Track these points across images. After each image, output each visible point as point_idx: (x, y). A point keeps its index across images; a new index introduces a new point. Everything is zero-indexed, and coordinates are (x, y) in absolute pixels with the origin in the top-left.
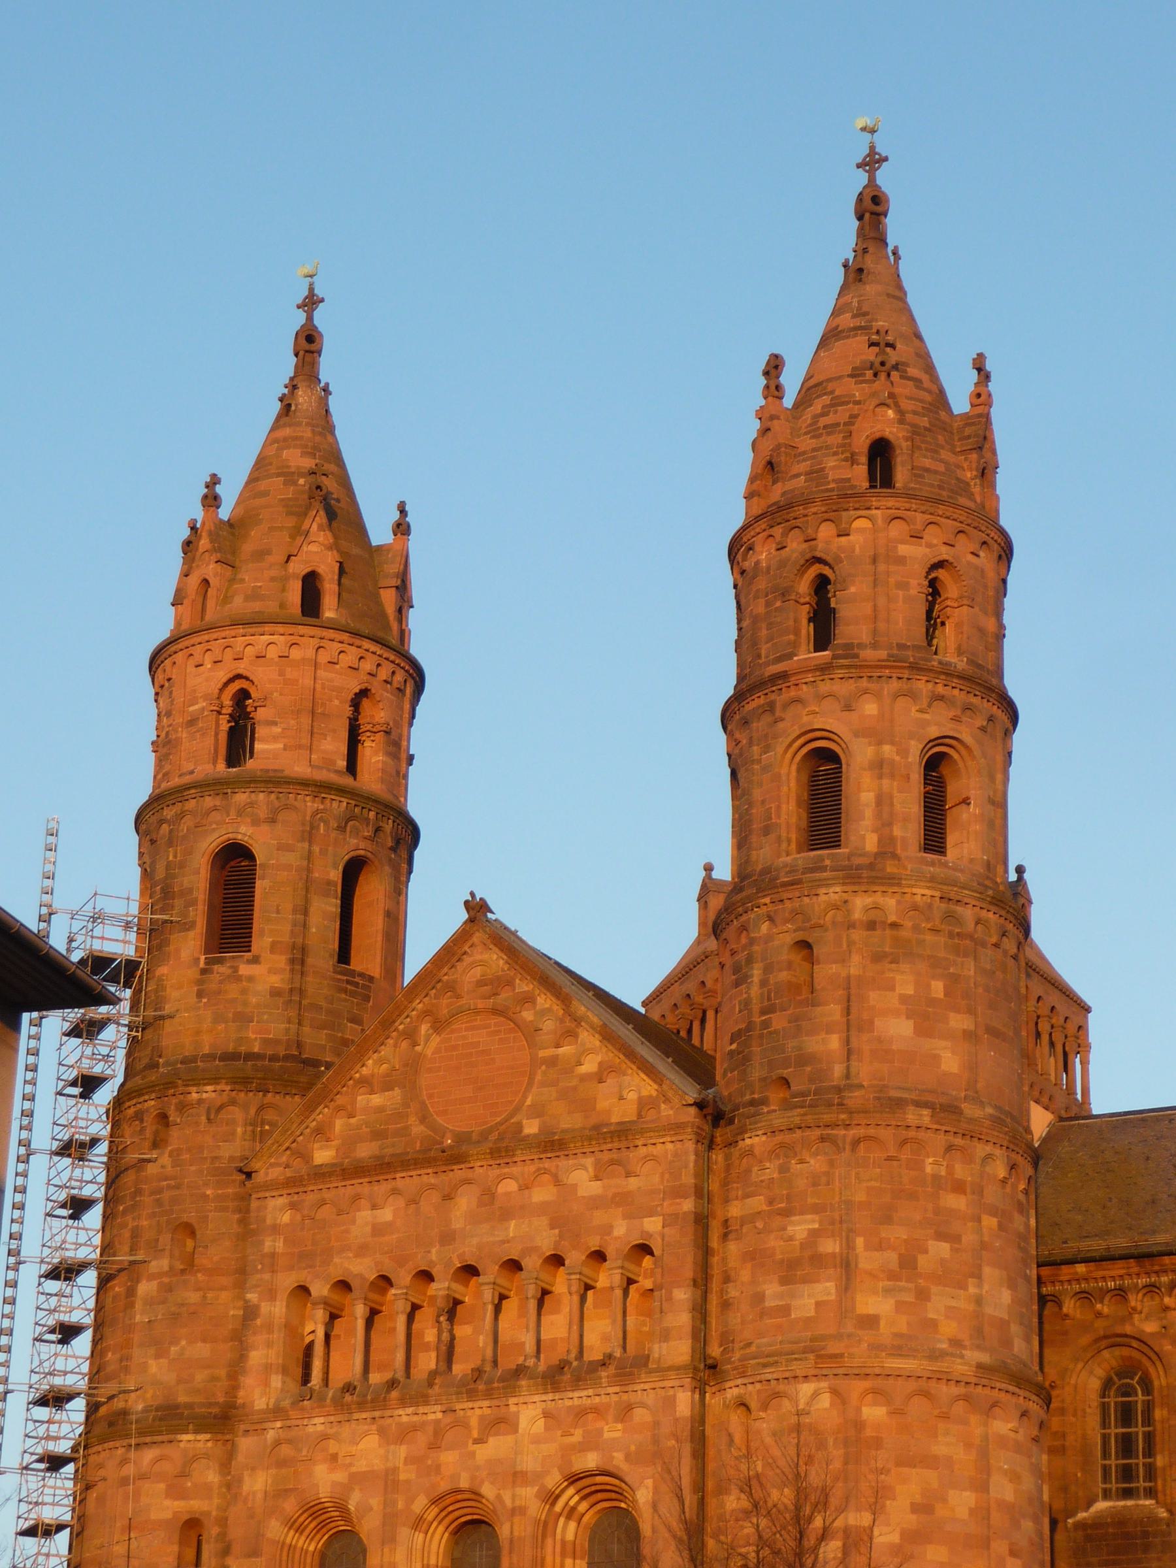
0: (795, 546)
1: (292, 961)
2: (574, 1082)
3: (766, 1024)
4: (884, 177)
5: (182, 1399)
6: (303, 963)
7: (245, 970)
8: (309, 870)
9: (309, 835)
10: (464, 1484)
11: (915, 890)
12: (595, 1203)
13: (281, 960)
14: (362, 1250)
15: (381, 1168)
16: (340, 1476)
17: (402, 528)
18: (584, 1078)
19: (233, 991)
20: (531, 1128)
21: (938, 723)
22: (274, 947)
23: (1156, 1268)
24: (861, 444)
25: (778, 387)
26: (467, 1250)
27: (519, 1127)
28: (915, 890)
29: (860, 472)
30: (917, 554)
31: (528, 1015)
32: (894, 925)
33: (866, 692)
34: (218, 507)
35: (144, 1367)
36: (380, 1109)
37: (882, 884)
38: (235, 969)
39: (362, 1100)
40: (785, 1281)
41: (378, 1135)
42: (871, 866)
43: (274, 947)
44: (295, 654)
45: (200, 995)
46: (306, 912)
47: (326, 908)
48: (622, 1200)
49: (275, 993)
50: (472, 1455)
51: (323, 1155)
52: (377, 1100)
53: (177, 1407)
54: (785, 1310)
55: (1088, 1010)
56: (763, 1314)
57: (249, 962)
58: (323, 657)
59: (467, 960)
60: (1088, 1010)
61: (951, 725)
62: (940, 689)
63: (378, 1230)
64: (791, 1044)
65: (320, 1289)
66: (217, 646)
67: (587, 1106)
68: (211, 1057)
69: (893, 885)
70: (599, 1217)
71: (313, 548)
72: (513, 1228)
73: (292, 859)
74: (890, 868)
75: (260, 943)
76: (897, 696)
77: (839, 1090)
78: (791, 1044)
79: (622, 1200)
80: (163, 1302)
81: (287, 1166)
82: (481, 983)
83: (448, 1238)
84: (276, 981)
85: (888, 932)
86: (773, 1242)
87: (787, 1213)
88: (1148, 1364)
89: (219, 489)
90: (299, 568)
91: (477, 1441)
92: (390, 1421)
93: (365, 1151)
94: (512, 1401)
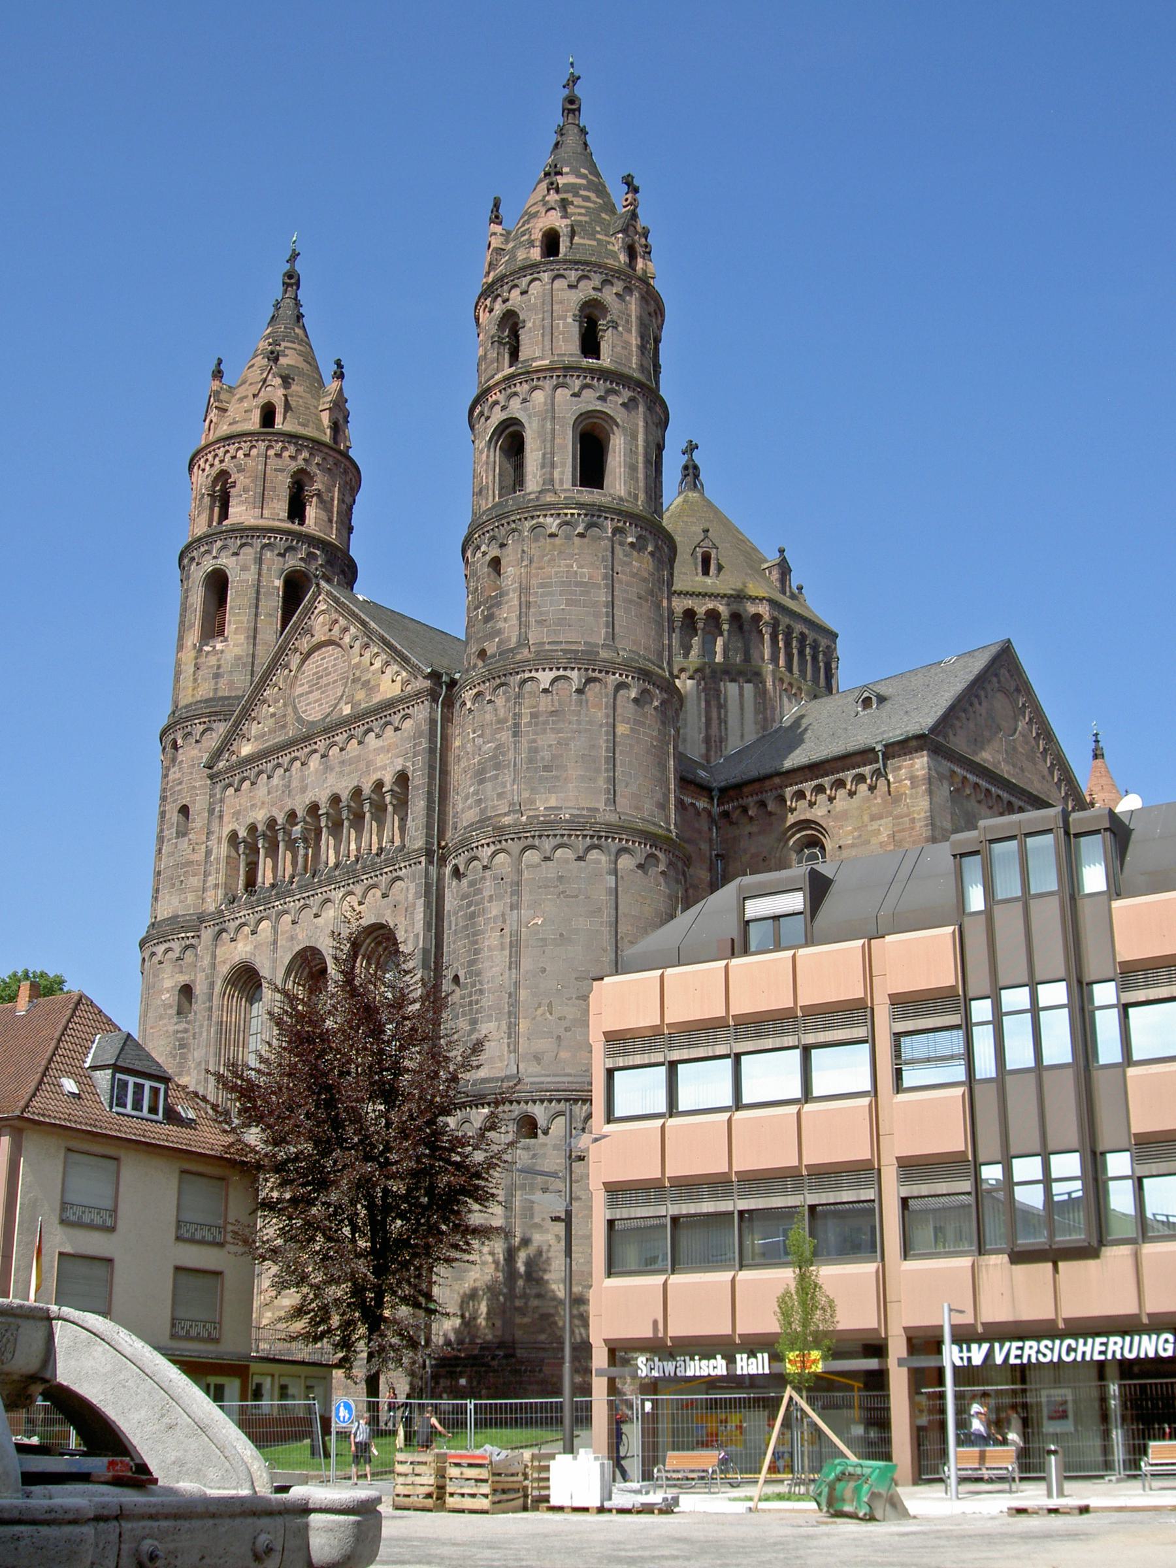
0: (499, 308)
1: (248, 638)
2: (370, 675)
4: (578, 90)
6: (255, 638)
7: (219, 646)
8: (259, 581)
9: (260, 561)
11: (566, 511)
12: (379, 751)
13: (241, 638)
17: (339, 375)
19: (213, 660)
20: (347, 710)
21: (590, 401)
22: (236, 631)
23: (822, 772)
24: (537, 235)
25: (497, 217)
28: (566, 511)
29: (536, 254)
30: (575, 298)
32: (552, 535)
33: (535, 388)
34: (222, 377)
37: (543, 510)
38: (214, 647)
42: (538, 498)
43: (236, 631)
44: (254, 452)
46: (257, 607)
47: (273, 603)
49: (238, 658)
51: (246, 750)
53: (178, 916)
55: (836, 636)
57: (222, 642)
58: (271, 452)
59: (316, 611)
60: (836, 636)
61: (599, 403)
62: (588, 380)
65: (242, 833)
66: (210, 457)
68: (200, 701)
69: (551, 509)
71: (269, 389)
73: (250, 576)
74: (549, 498)
75: (229, 629)
76: (556, 387)
77: (512, 650)
81: (227, 761)
82: (324, 624)
84: (238, 651)
85: (548, 540)
88: (822, 837)
89: (222, 367)
90: (261, 401)
91: (316, 916)
92: (272, 910)
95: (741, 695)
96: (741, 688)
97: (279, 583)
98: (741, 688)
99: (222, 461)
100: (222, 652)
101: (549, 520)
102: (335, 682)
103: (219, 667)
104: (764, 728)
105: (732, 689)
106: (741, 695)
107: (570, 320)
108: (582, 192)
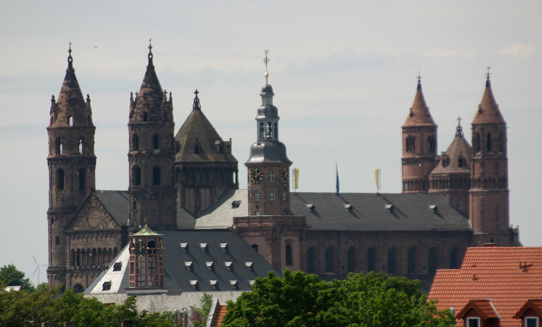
7: (63, 192)
27: (100, 227)
32: (148, 199)
38: (62, 192)
95: (206, 192)
96: (206, 190)
97: (77, 173)
98: (206, 190)
99: (58, 134)
100: (64, 194)
101: (147, 195)
102: (98, 218)
103: (64, 198)
104: (212, 202)
105: (203, 191)
106: (206, 192)
107: (150, 140)
108: (153, 95)
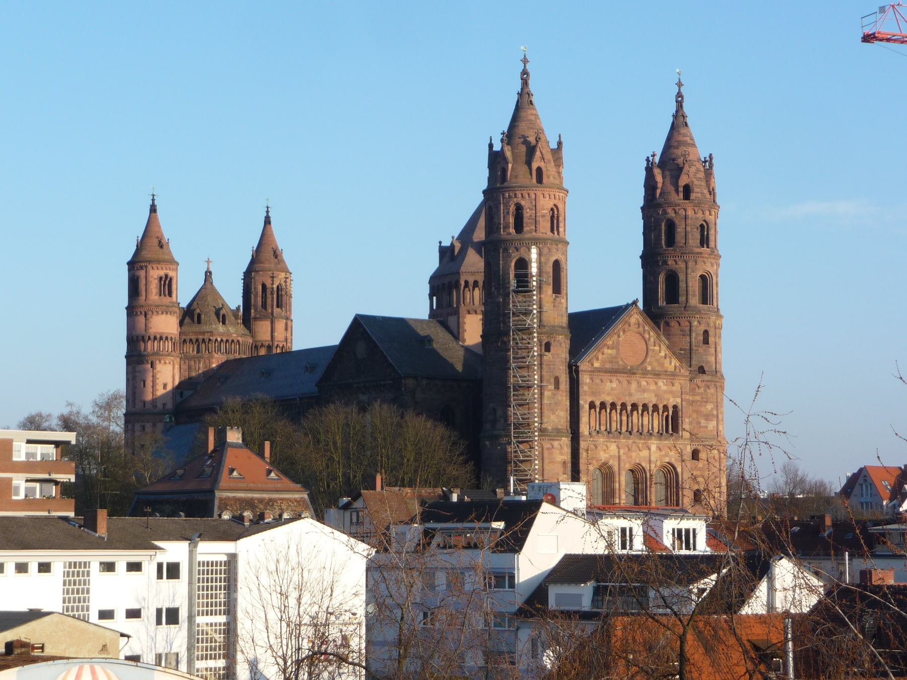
3: (697, 350)
5: (560, 427)
10: (638, 462)
12: (665, 392)
14: (609, 394)
15: (614, 372)
16: (607, 456)
18: (661, 357)
26: (634, 399)
31: (647, 336)
35: (549, 417)
36: (611, 355)
39: (606, 351)
40: (706, 420)
41: (611, 362)
45: (554, 306)
48: (671, 392)
50: (639, 454)
52: (610, 351)
54: (706, 427)
56: (700, 427)
63: (612, 389)
64: (704, 357)
67: (662, 365)
70: (667, 396)
72: (646, 395)
78: (704, 357)
79: (671, 392)
80: (553, 398)
83: (630, 395)
86: (703, 409)
87: (706, 402)
93: (608, 366)
94: (649, 442)
